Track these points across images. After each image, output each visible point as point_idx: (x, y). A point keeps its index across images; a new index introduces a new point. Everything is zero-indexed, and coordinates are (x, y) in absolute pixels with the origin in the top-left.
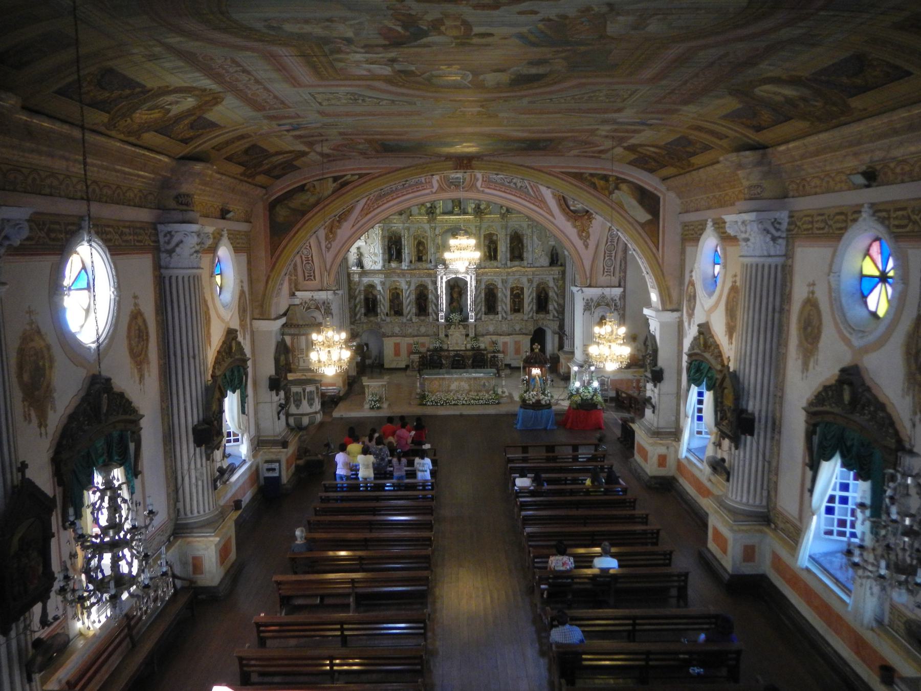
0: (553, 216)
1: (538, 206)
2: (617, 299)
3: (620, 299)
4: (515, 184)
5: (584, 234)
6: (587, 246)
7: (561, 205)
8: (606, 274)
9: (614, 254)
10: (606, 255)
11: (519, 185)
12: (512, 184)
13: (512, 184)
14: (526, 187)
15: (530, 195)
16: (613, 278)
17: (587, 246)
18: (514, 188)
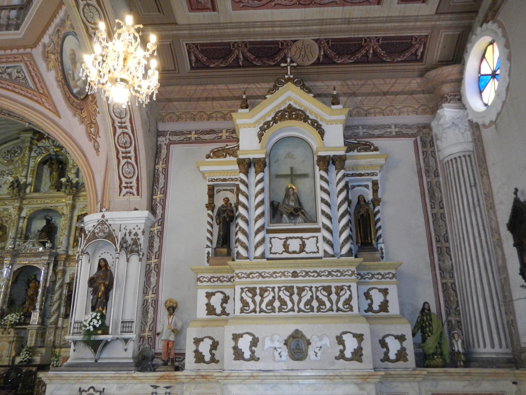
0: (57, 113)
1: (37, 101)
2: (140, 232)
3: (143, 232)
4: (10, 74)
5: (93, 130)
6: (97, 150)
7: (66, 94)
8: (124, 191)
9: (132, 154)
10: (121, 155)
11: (15, 75)
12: (5, 76)
13: (5, 76)
14: (25, 77)
15: (31, 89)
16: (138, 198)
17: (97, 150)
18: (5, 80)
